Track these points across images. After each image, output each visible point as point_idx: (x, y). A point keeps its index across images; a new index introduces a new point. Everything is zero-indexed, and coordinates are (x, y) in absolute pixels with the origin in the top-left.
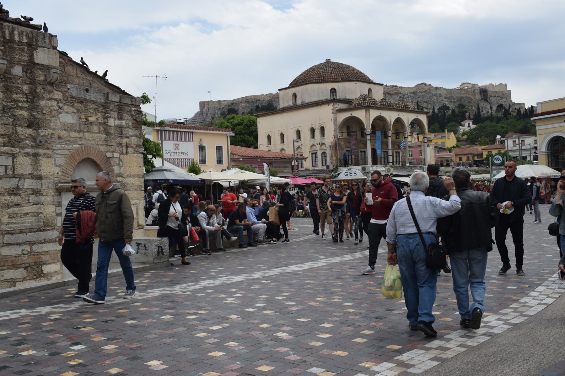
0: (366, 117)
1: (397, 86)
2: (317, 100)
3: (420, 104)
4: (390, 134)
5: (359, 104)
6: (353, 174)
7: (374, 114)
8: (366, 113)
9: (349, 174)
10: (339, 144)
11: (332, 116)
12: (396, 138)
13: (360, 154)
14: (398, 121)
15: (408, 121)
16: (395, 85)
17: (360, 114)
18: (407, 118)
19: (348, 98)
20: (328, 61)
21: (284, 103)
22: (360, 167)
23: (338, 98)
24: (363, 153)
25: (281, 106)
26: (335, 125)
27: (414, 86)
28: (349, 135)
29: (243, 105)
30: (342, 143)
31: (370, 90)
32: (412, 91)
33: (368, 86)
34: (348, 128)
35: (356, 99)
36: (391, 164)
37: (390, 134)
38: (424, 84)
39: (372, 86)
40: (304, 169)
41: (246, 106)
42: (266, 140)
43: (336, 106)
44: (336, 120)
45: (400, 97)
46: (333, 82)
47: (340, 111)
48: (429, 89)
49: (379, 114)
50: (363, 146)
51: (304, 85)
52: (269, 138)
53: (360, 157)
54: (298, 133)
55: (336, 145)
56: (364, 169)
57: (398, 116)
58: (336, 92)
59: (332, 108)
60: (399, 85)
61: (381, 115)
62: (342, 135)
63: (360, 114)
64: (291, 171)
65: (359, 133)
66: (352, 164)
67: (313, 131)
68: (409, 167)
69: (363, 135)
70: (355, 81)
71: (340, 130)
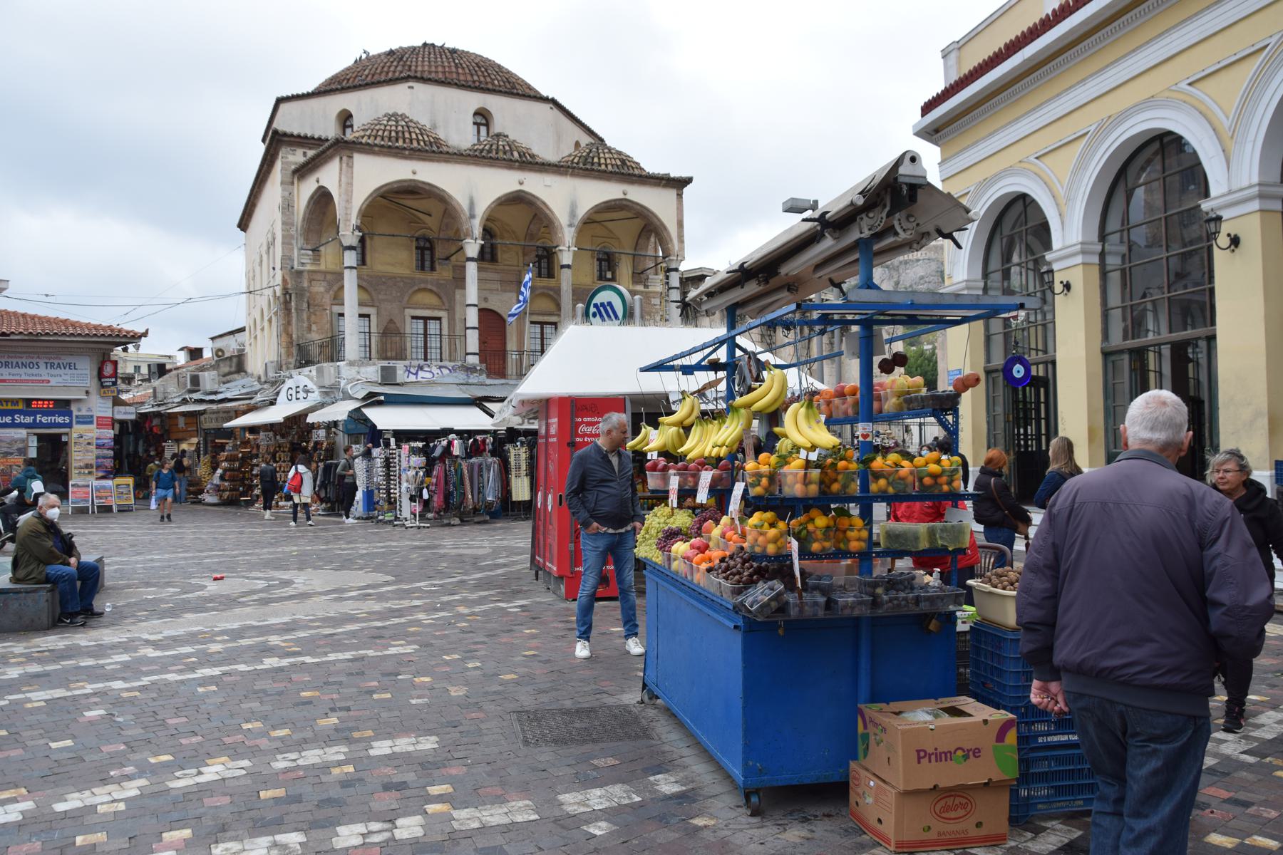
6: (302, 395)
9: (293, 392)
10: (301, 293)
26: (287, 224)
30: (319, 288)
31: (483, 118)
33: (475, 100)
43: (291, 158)
44: (287, 207)
49: (411, 177)
55: (286, 292)
61: (417, 177)
64: (92, 384)
71: (307, 240)
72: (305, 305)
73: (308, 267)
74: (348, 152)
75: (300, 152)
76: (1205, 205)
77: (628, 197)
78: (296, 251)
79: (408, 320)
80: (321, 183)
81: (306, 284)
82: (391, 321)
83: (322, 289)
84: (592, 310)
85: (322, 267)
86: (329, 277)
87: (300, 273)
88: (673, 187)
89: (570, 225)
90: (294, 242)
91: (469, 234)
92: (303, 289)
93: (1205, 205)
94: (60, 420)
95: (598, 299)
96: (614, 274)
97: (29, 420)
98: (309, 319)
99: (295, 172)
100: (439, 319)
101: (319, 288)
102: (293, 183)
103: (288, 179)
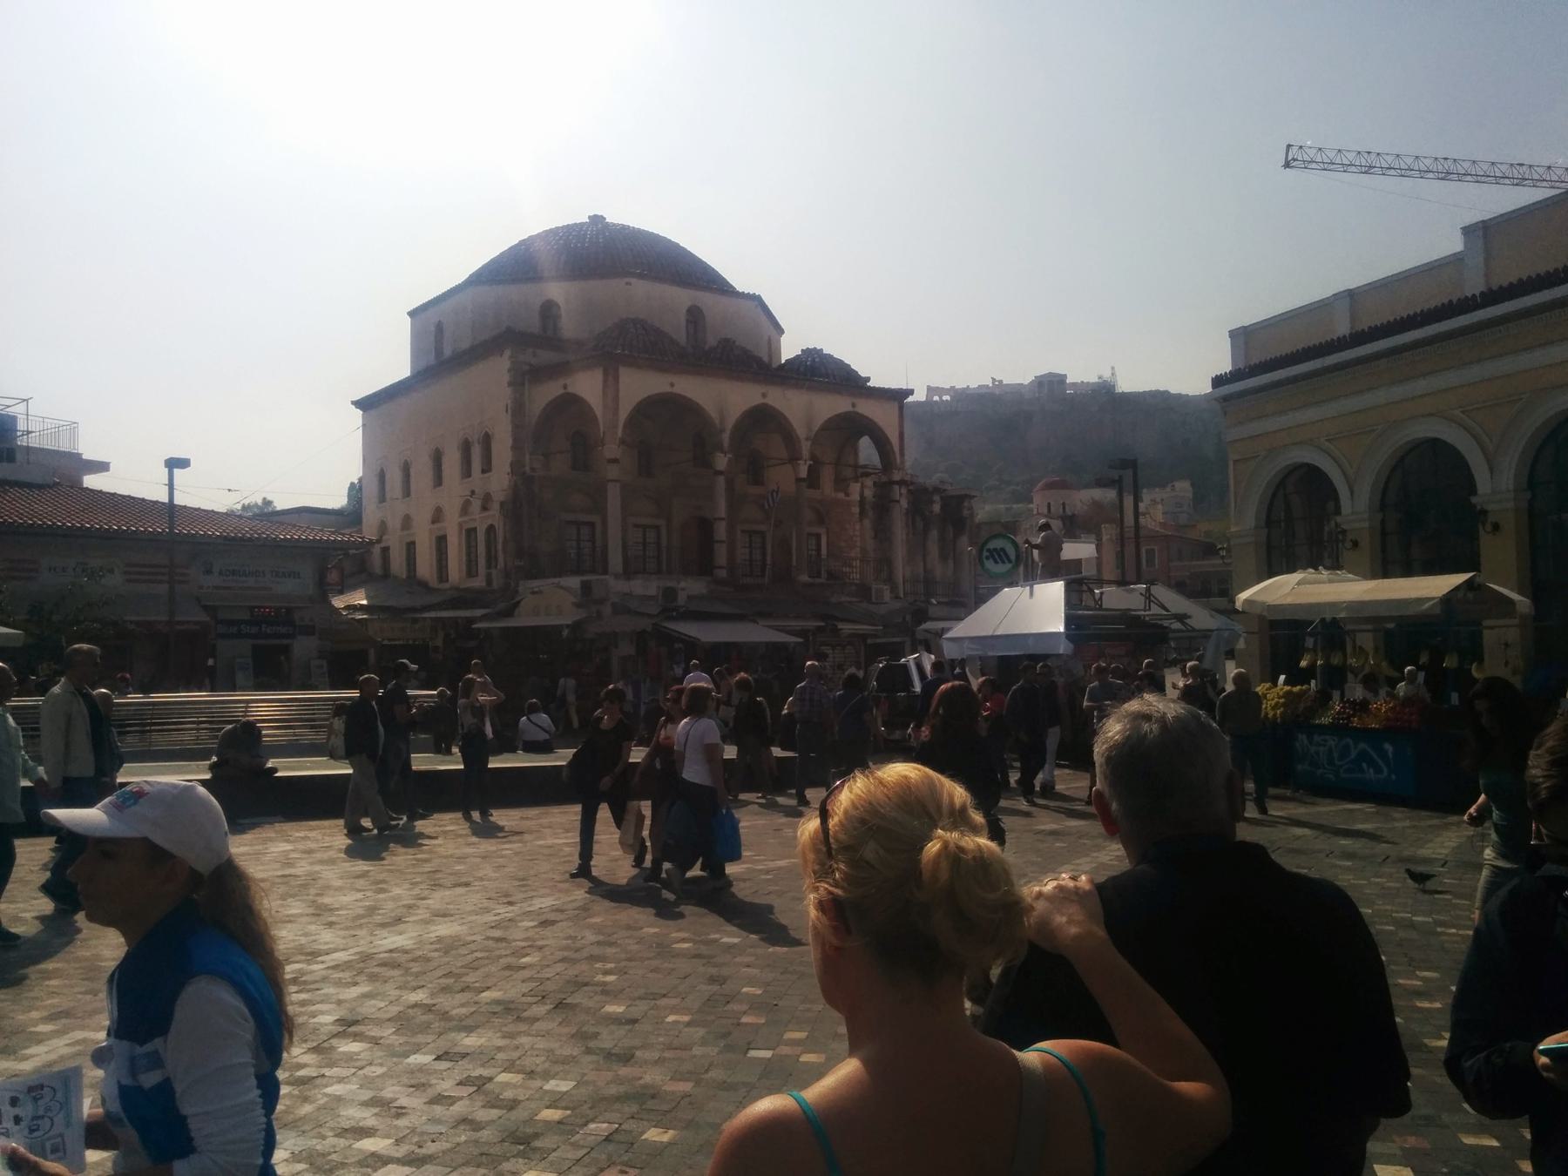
0: (604, 393)
7: (639, 385)
8: (605, 381)
11: (504, 395)
14: (762, 419)
17: (587, 385)
22: (574, 582)
26: (517, 427)
37: (722, 461)
40: (446, 586)
44: (518, 410)
49: (669, 389)
54: (437, 459)
56: (586, 588)
57: (758, 400)
61: (677, 390)
67: (466, 447)
76: (1474, 500)
80: (570, 390)
84: (985, 554)
93: (1474, 500)
94: (283, 630)
95: (991, 545)
97: (254, 630)
100: (657, 528)
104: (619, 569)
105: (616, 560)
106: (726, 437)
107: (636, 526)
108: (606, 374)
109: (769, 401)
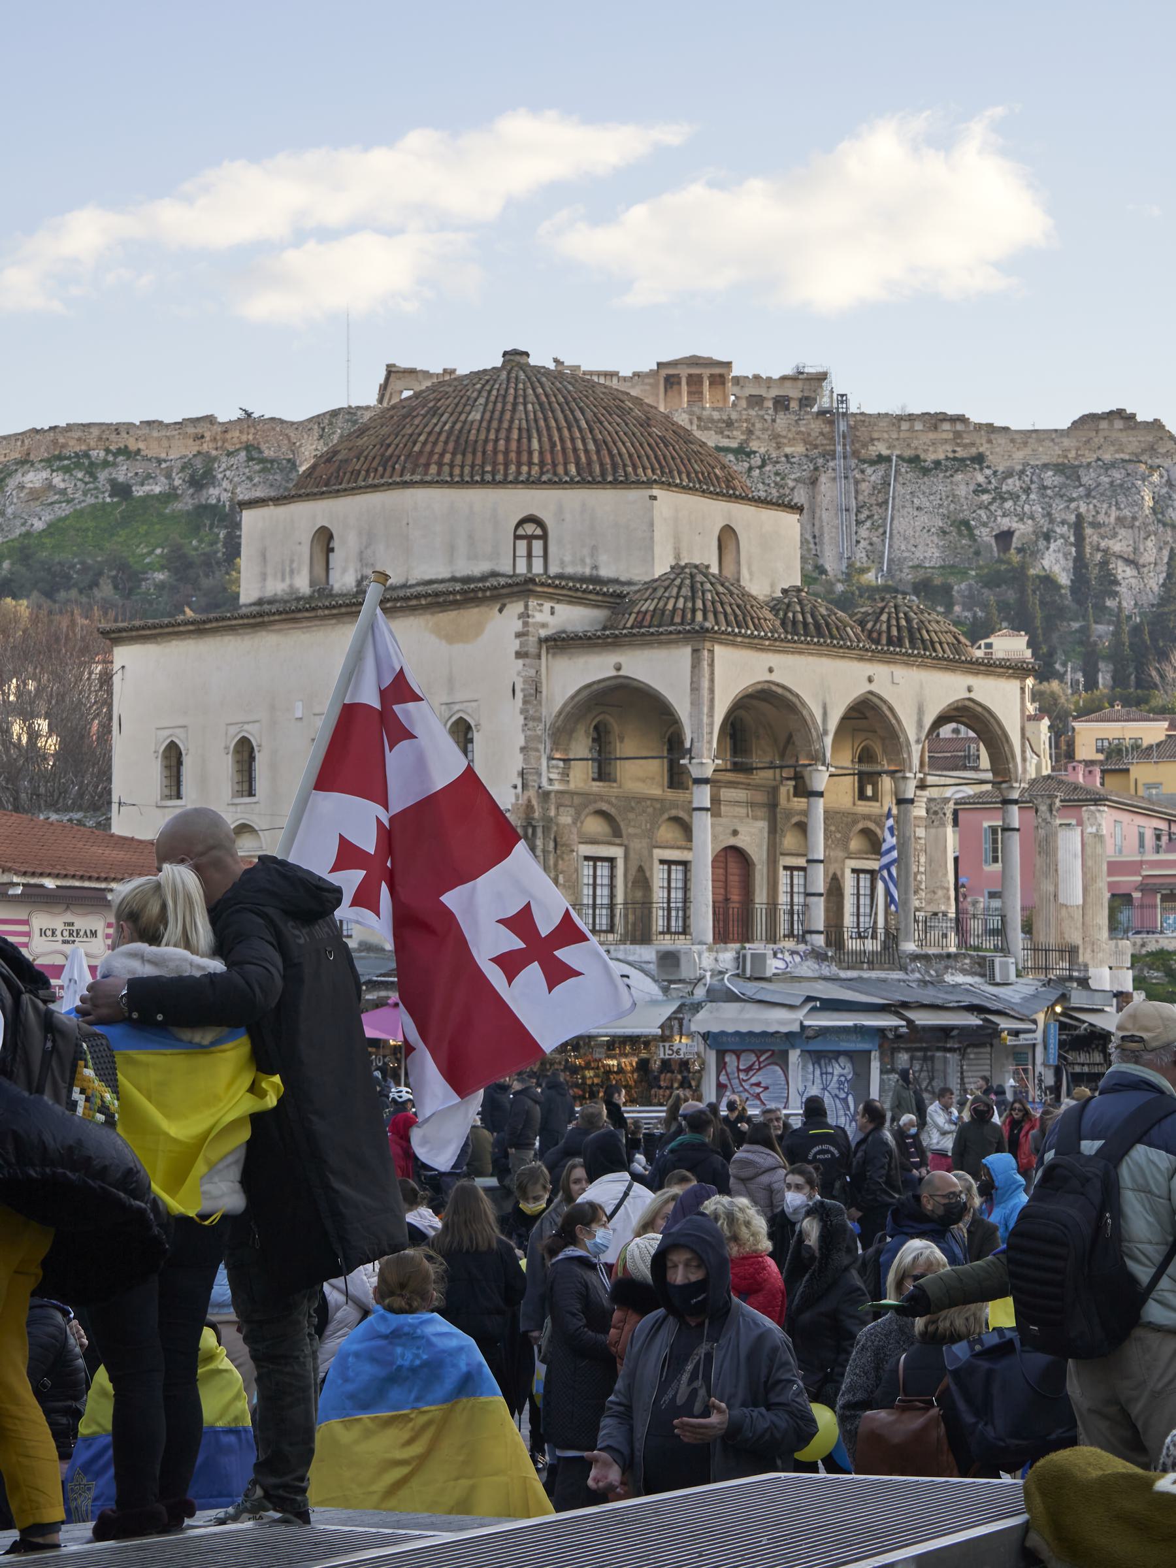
0: (695, 688)
1: (962, 419)
2: (445, 573)
3: (1088, 531)
4: (821, 779)
5: (659, 616)
7: (736, 670)
8: (696, 665)
10: (548, 822)
11: (515, 671)
12: (862, 796)
13: (658, 875)
15: (921, 712)
16: (951, 411)
17: (660, 669)
18: (916, 693)
19: (604, 573)
20: (515, 358)
21: (264, 577)
23: (553, 570)
24: (677, 873)
25: (249, 591)
27: (1065, 425)
28: (603, 774)
29: (34, 478)
31: (727, 537)
32: (1049, 454)
33: (716, 512)
34: (601, 738)
35: (652, 586)
36: (820, 940)
38: (1120, 414)
39: (742, 515)
41: (50, 486)
42: (155, 771)
44: (534, 691)
45: (980, 490)
46: (530, 483)
47: (562, 643)
48: (1152, 449)
50: (667, 833)
51: (375, 488)
52: (173, 757)
53: (659, 895)
58: (544, 537)
59: (518, 626)
60: (976, 417)
61: (774, 677)
62: (565, 774)
63: (660, 669)
65: (656, 768)
66: (611, 929)
68: (916, 957)
69: (677, 778)
70: (649, 484)
71: (556, 745)
72: (552, 844)
73: (557, 787)
74: (708, 645)
75: (547, 606)
77: (972, 695)
78: (544, 762)
79: (656, 863)
80: (621, 673)
81: (552, 813)
82: (641, 869)
83: (569, 820)
85: (572, 786)
86: (577, 800)
87: (545, 796)
88: (1017, 678)
89: (918, 741)
90: (542, 747)
91: (818, 758)
92: (550, 820)
96: (875, 791)
98: (556, 865)
99: (547, 639)
101: (566, 819)
102: (539, 657)
103: (533, 650)
104: (710, 938)
105: (704, 920)
106: (829, 740)
107: (662, 862)
108: (695, 651)
109: (873, 687)
